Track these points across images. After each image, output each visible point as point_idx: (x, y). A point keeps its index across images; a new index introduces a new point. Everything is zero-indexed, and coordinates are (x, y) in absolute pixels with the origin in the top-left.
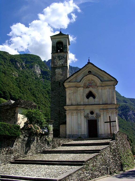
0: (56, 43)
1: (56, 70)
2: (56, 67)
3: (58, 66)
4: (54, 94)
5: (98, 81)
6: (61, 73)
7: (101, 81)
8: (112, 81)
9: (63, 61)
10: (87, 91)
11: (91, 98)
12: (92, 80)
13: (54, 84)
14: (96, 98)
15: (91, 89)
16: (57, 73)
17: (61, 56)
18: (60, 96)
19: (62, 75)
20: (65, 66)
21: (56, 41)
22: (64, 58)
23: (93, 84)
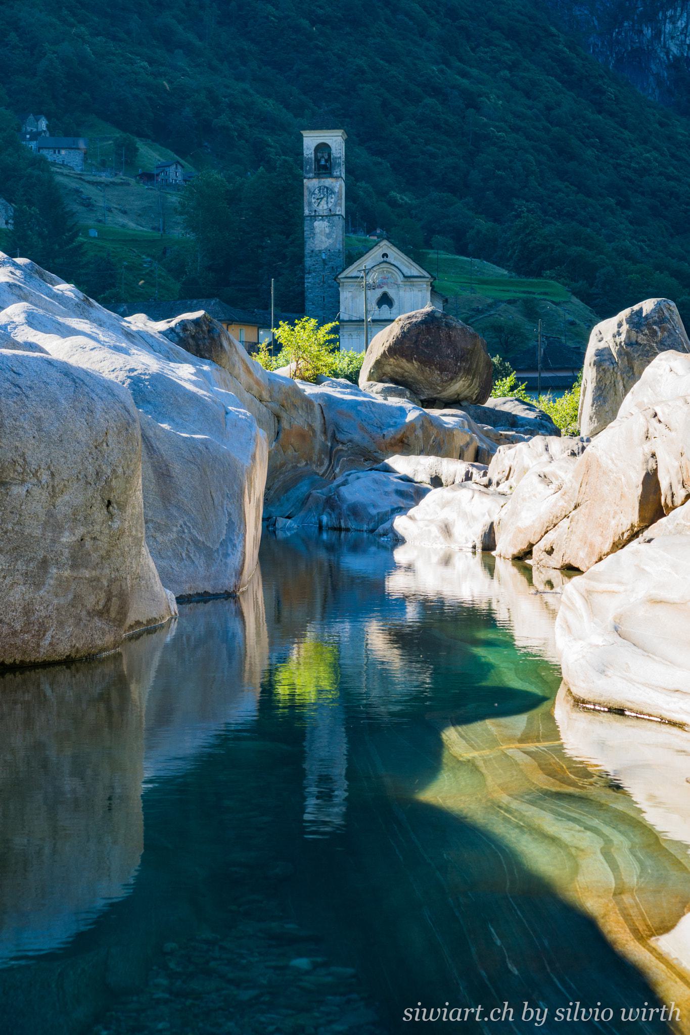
0: (313, 148)
1: (316, 224)
2: (315, 216)
3: (321, 213)
4: (313, 281)
5: (400, 278)
6: (327, 230)
7: (405, 277)
8: (424, 277)
9: (332, 200)
10: (378, 293)
11: (385, 307)
12: (390, 272)
13: (311, 256)
14: (395, 306)
15: (385, 289)
16: (317, 230)
17: (327, 188)
18: (326, 285)
19: (328, 236)
20: (336, 215)
21: (315, 145)
22: (333, 193)
23: (389, 281)
